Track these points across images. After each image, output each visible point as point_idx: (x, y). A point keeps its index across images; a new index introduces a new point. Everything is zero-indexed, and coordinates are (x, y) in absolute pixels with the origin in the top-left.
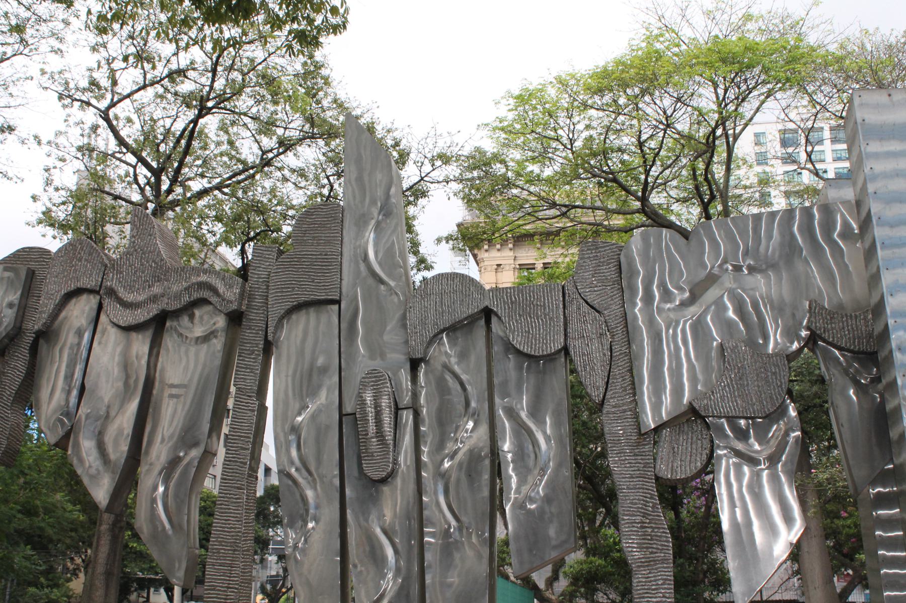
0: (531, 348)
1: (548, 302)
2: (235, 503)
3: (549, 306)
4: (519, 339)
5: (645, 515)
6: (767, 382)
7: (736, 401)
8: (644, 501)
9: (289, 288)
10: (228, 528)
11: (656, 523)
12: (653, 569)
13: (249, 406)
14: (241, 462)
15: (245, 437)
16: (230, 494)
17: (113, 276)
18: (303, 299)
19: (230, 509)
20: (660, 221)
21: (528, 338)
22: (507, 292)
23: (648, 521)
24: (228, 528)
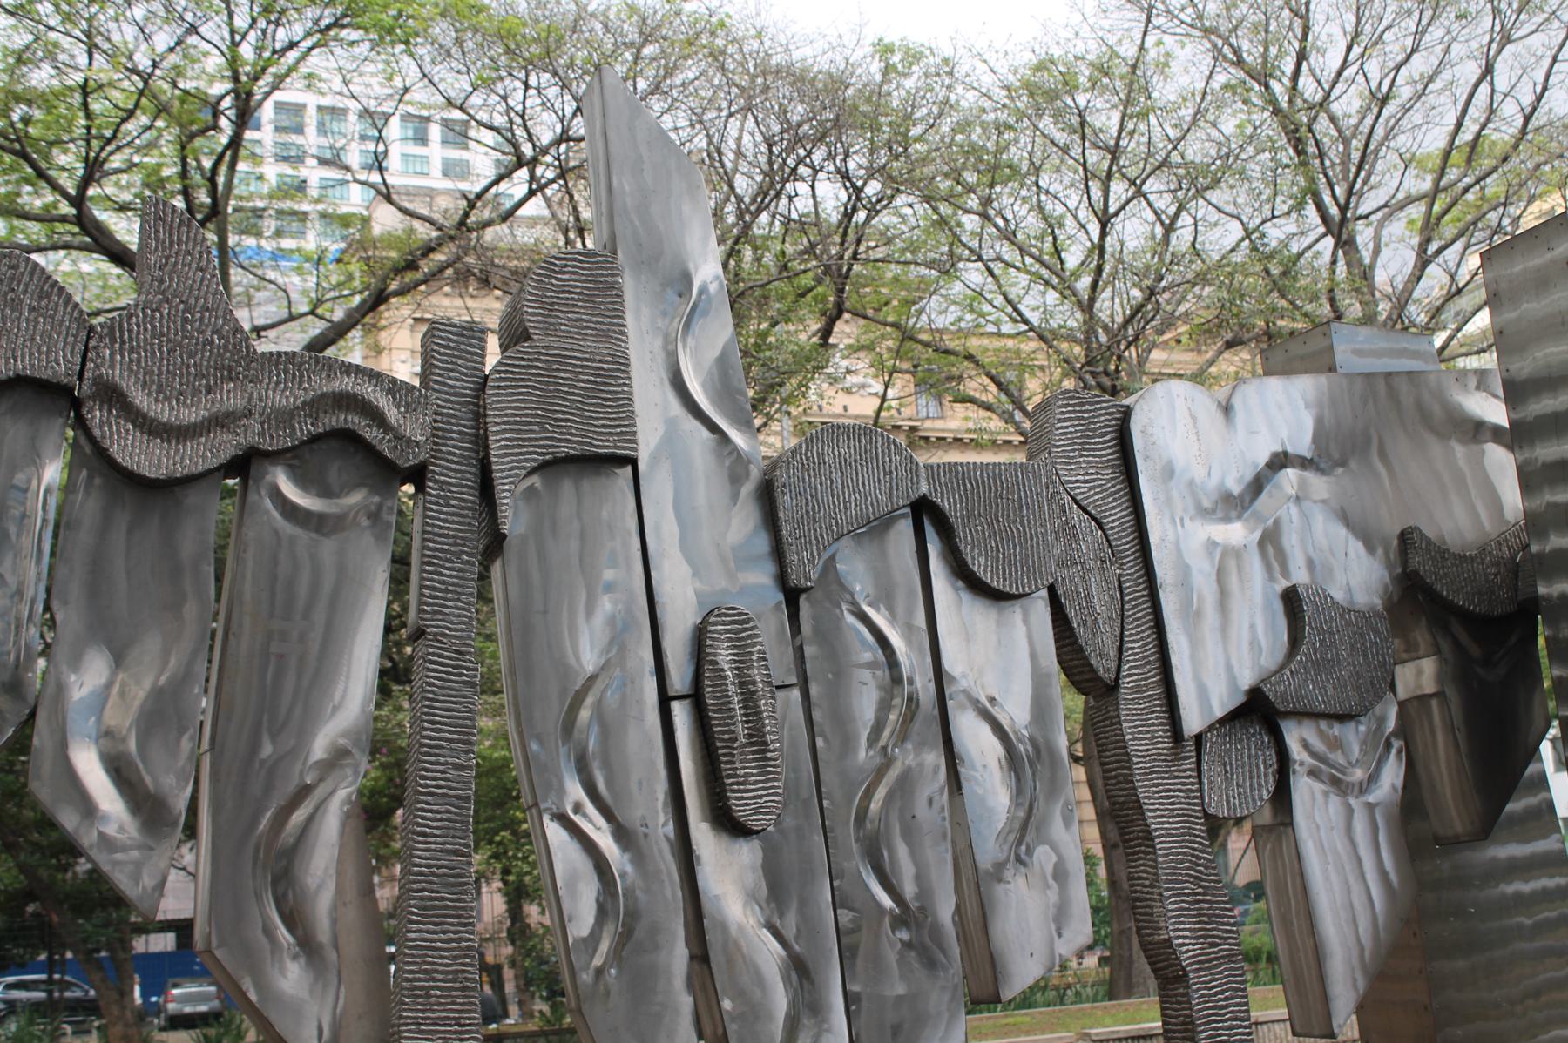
0: (1005, 580)
1: (1026, 497)
2: (453, 885)
3: (1027, 504)
4: (982, 560)
5: (1197, 880)
6: (1365, 655)
7: (1324, 687)
8: (1193, 856)
9: (530, 423)
10: (442, 941)
11: (1213, 895)
12: (1217, 973)
13: (461, 675)
14: (458, 797)
15: (459, 741)
16: (439, 867)
17: (112, 355)
18: (564, 451)
19: (443, 899)
20: (106, 242)
21: (998, 561)
22: (957, 472)
23: (1200, 890)
24: (442, 941)
